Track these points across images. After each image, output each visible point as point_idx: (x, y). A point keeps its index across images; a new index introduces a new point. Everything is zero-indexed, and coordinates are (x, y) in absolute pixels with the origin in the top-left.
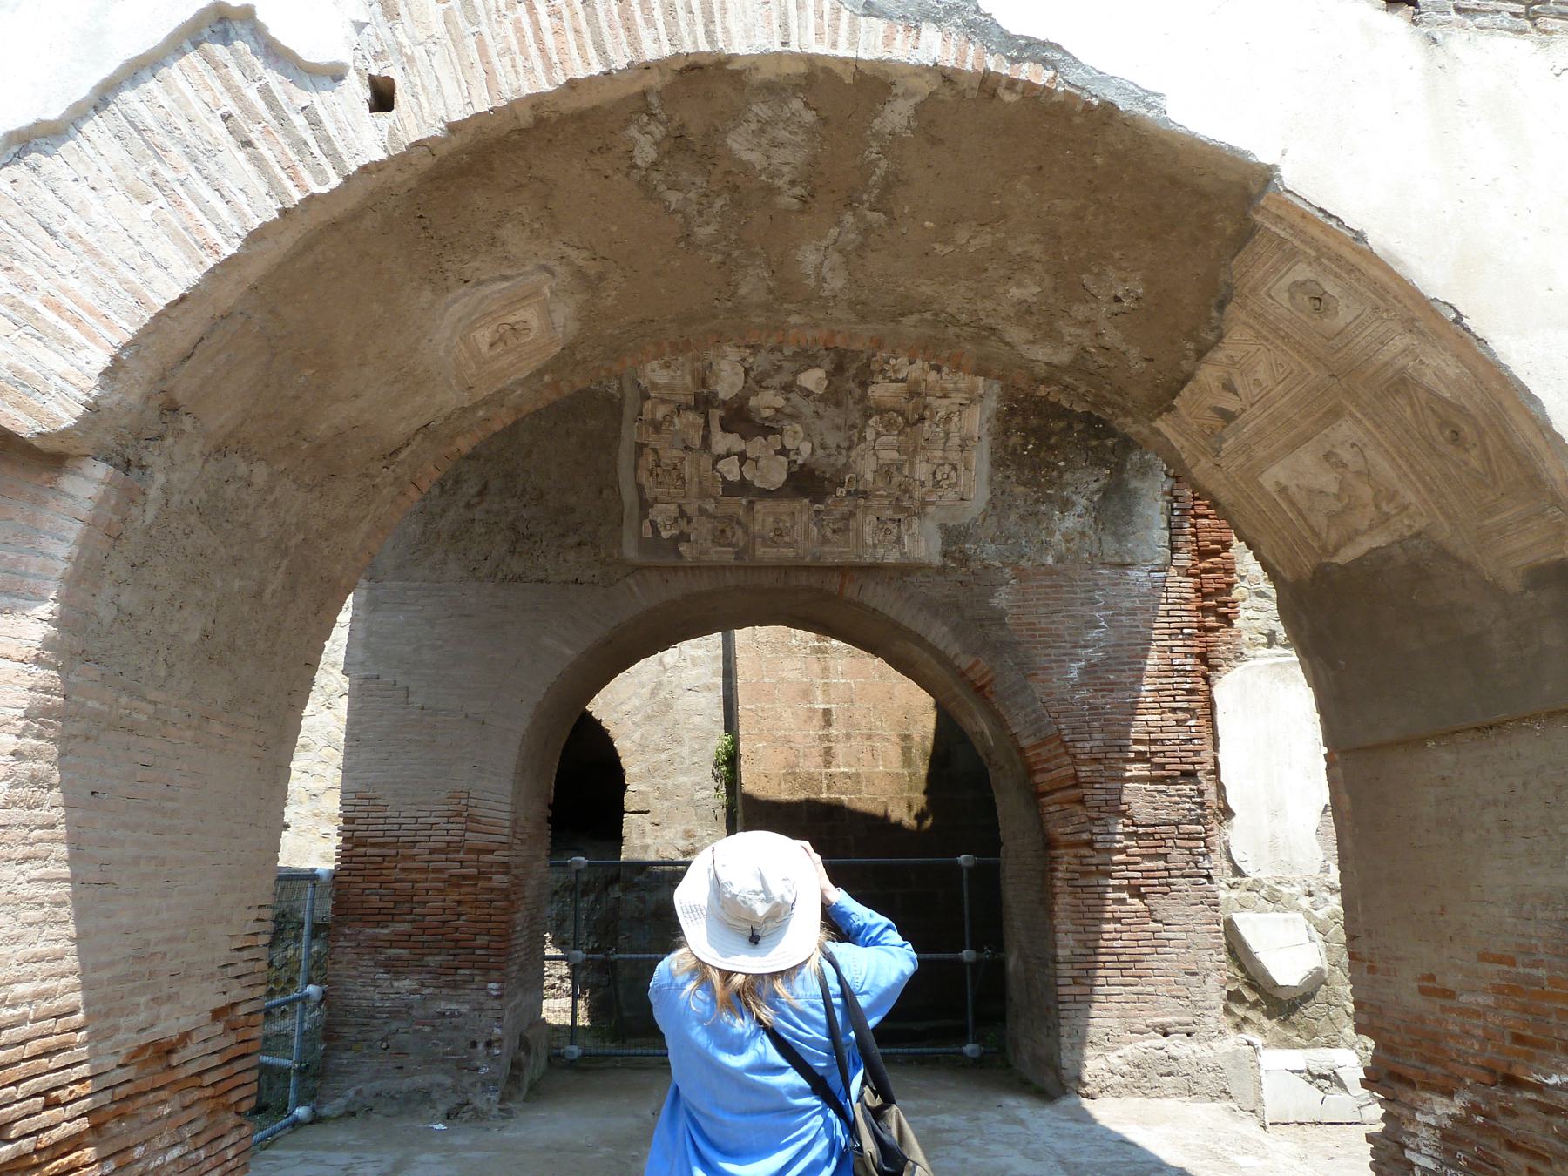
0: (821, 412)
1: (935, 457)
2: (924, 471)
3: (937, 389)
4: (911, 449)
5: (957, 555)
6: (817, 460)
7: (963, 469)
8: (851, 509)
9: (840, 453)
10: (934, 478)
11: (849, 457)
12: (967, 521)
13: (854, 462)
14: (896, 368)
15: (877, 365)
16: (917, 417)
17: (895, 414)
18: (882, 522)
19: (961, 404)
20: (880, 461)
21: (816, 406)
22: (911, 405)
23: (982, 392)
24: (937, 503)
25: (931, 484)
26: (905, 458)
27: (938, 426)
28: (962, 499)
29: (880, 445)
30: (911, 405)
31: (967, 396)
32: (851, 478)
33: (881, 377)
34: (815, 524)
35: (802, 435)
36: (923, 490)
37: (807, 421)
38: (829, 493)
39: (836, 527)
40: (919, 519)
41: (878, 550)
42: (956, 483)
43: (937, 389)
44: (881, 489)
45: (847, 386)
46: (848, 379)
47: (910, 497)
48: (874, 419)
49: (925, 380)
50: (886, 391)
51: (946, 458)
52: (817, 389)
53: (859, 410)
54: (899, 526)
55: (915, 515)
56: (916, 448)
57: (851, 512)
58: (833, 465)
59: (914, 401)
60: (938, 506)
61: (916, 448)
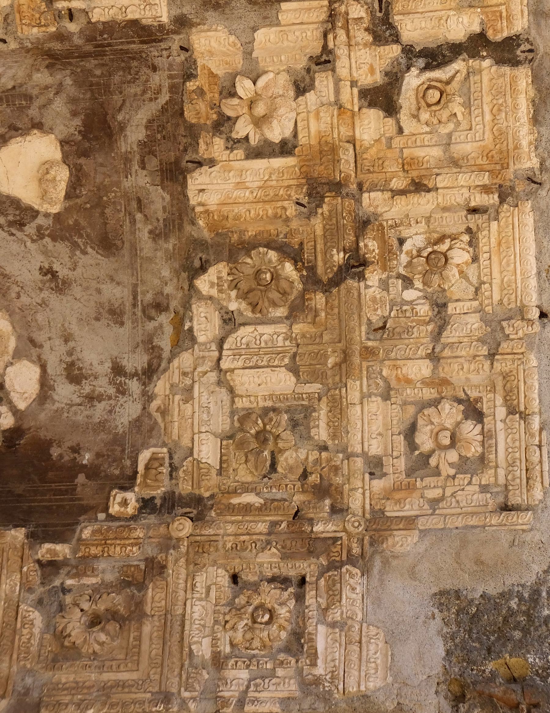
0: (63, 272)
1: (408, 381)
2: (377, 426)
3: (392, 167)
4: (331, 362)
5: (498, 691)
6: (59, 412)
7: (501, 412)
8: (150, 551)
9: (122, 391)
10: (412, 446)
11: (148, 397)
12: (530, 579)
13: (164, 412)
14: (260, 109)
15: (202, 106)
16: (339, 257)
17: (272, 255)
18: (248, 585)
19: (474, 211)
20: (240, 404)
21: (45, 252)
22: (318, 224)
23: (535, 163)
24: (422, 524)
25: (402, 464)
26: (315, 388)
27: (408, 282)
28: (506, 508)
29: (237, 355)
30: (318, 224)
31: (485, 179)
32: (154, 458)
33: (219, 142)
34: (40, 602)
35: (12, 344)
36: (378, 485)
37: (24, 299)
38: (85, 510)
39: (102, 607)
40: (366, 571)
41: (230, 674)
42: (482, 459)
43: (392, 167)
44: (246, 488)
45: (127, 183)
46: (127, 160)
47: (335, 510)
48: (212, 273)
49: (352, 141)
50: (240, 185)
51: (445, 382)
52: (44, 195)
53: (170, 257)
54: (300, 598)
55: (351, 560)
56: (346, 356)
57: (150, 561)
58: (102, 426)
59: (325, 208)
60: (424, 533)
61: (346, 356)
